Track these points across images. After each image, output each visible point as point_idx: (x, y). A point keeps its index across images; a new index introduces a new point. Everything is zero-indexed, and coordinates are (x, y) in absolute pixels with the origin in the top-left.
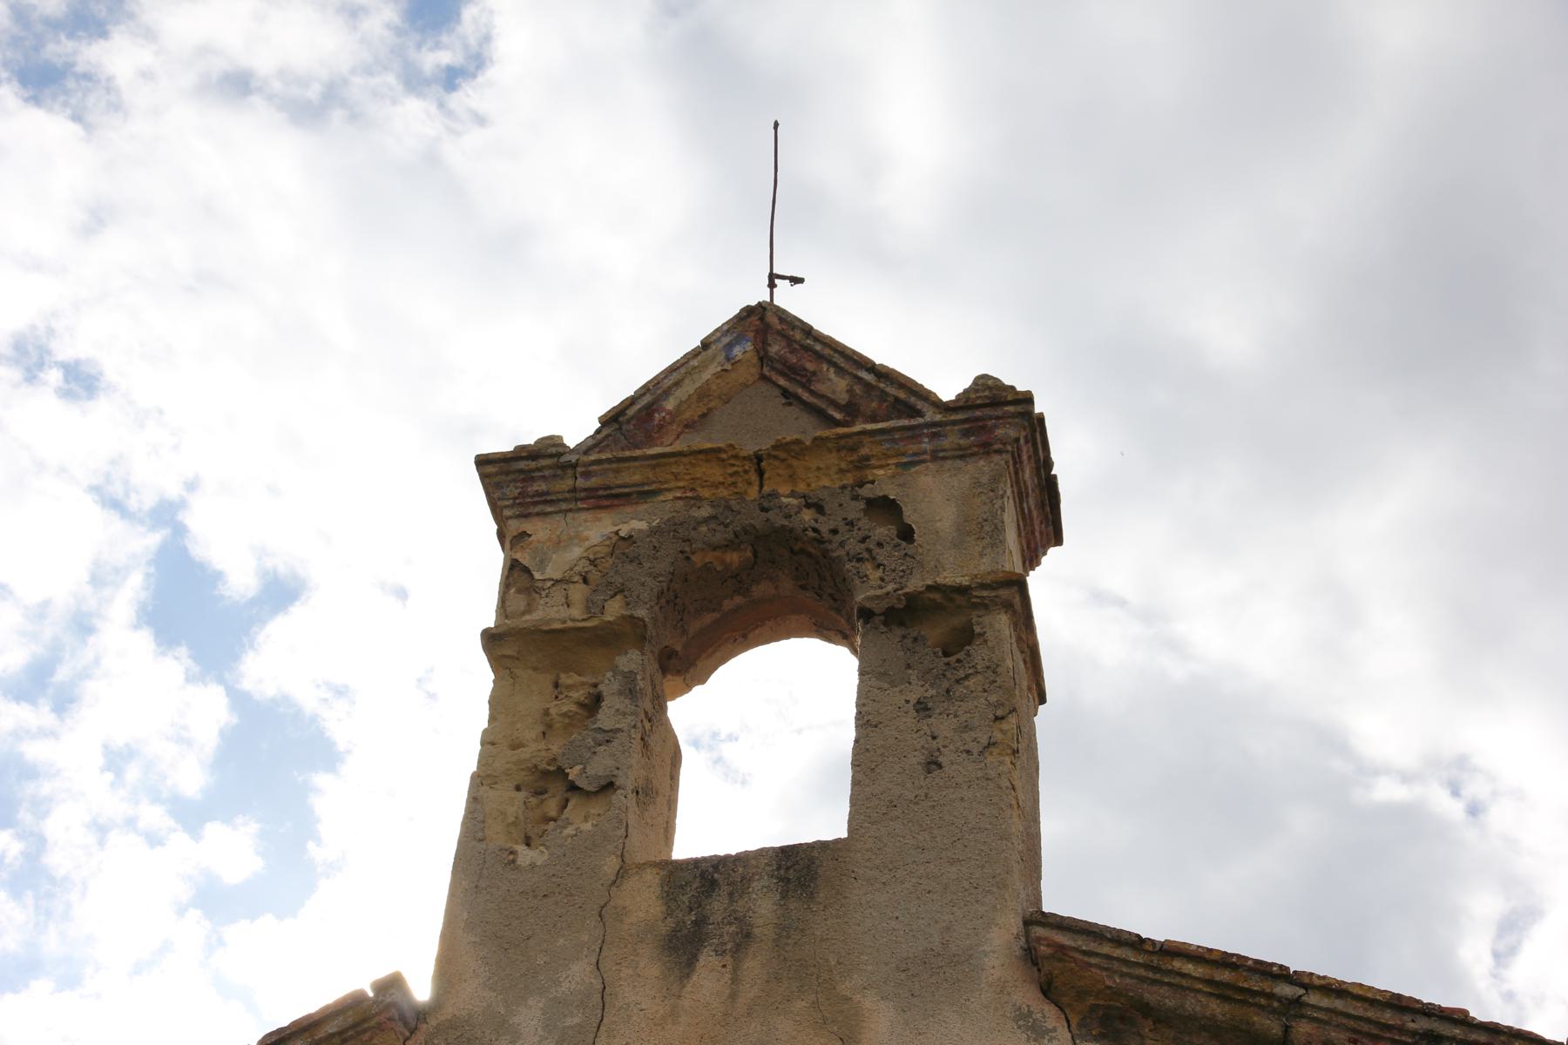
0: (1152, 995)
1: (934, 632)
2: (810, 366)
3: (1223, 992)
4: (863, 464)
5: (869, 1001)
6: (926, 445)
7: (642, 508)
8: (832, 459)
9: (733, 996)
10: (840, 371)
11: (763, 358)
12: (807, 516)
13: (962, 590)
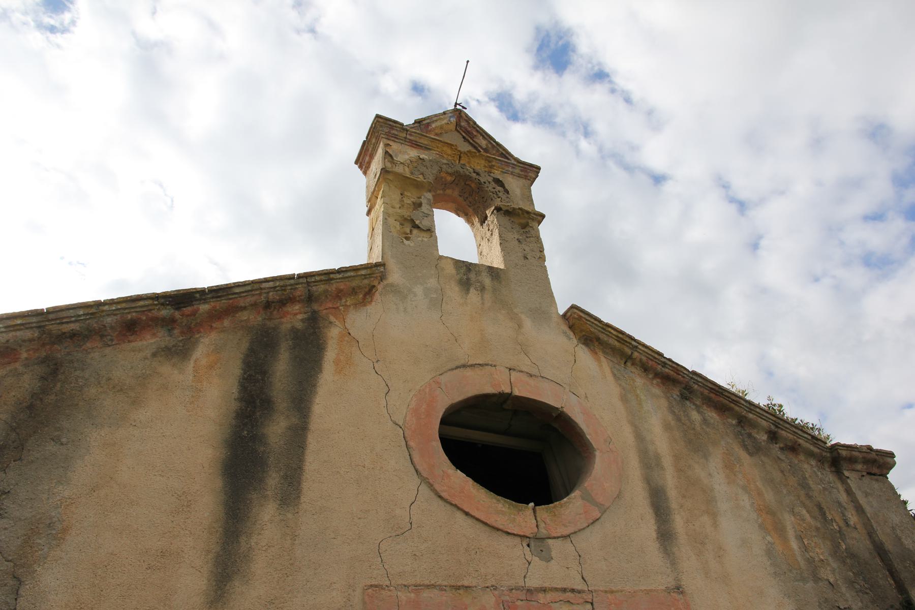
0: (602, 336)
2: (475, 133)
3: (619, 340)
4: (492, 167)
5: (523, 316)
6: (510, 169)
7: (426, 152)
8: (483, 162)
9: (483, 304)
11: (458, 124)
12: (474, 175)
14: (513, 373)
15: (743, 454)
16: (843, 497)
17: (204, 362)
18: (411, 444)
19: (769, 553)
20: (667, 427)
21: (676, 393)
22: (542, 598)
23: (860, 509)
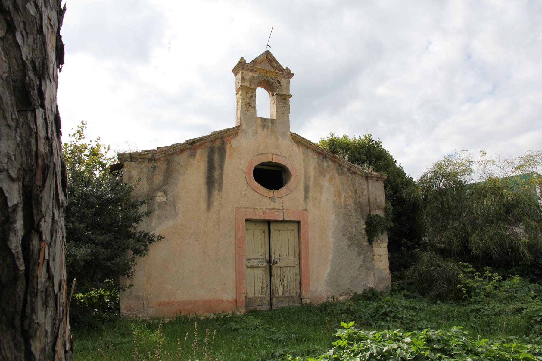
0: (301, 142)
1: (282, 97)
2: (273, 61)
3: (306, 143)
4: (277, 75)
5: (279, 136)
6: (283, 76)
7: (255, 73)
8: (274, 74)
9: (268, 133)
10: (276, 63)
11: (267, 57)
12: (271, 79)
13: (287, 95)
14: (273, 155)
15: (337, 176)
16: (365, 187)
17: (199, 158)
18: (246, 176)
19: (334, 202)
20: (315, 168)
21: (321, 157)
22: (272, 211)
23: (369, 191)
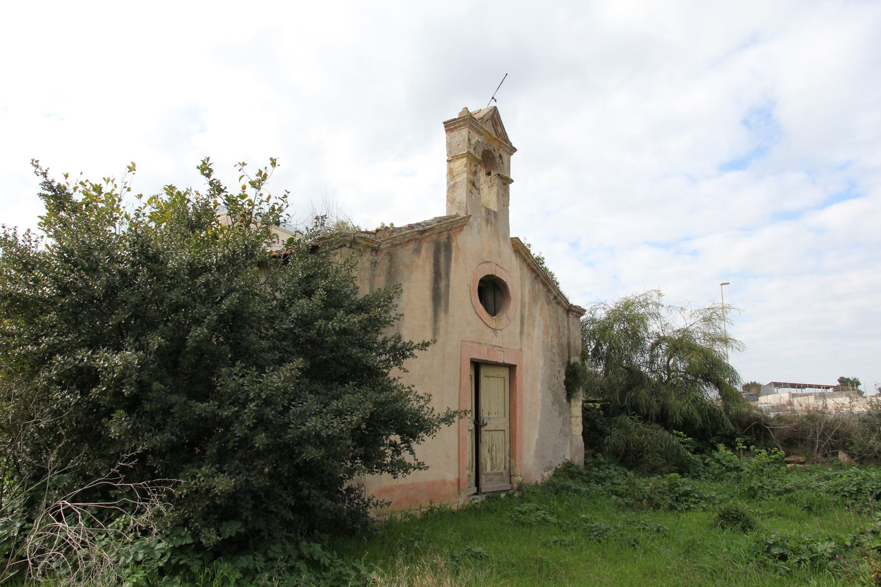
3: (526, 254)
4: (500, 147)
11: (493, 115)
14: (497, 267)
15: (546, 305)
16: (566, 324)
17: (424, 256)
18: (472, 293)
19: (543, 342)
20: (529, 292)
21: (534, 276)
22: (495, 348)
23: (569, 329)
